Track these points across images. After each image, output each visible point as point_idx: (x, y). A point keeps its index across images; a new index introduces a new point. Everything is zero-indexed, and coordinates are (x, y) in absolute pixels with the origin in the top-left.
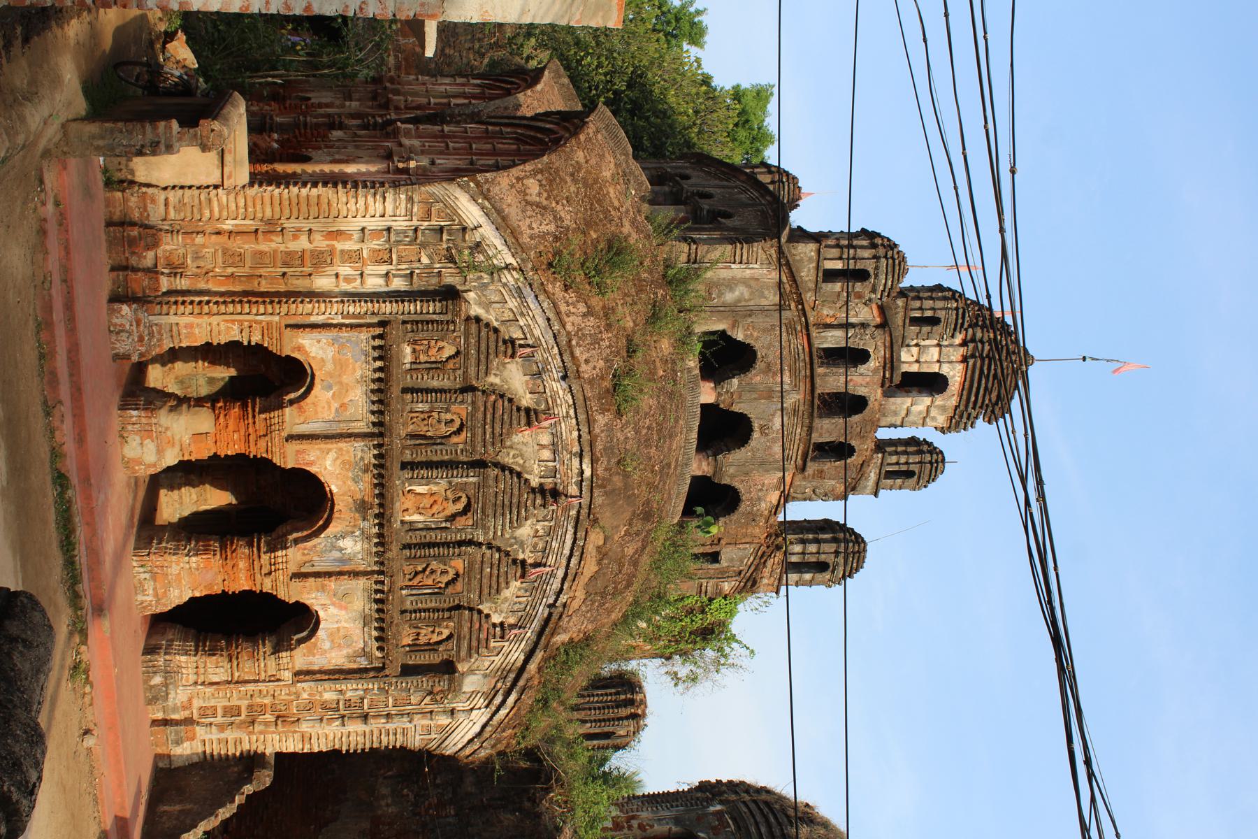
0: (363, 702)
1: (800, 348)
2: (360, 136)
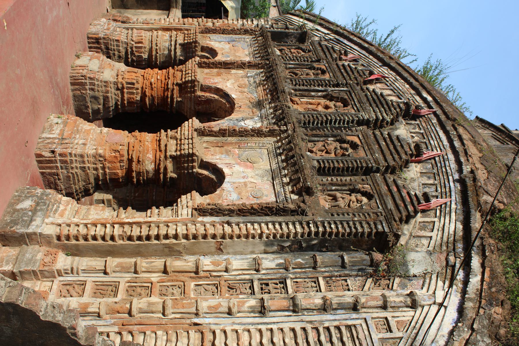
0: (285, 287)
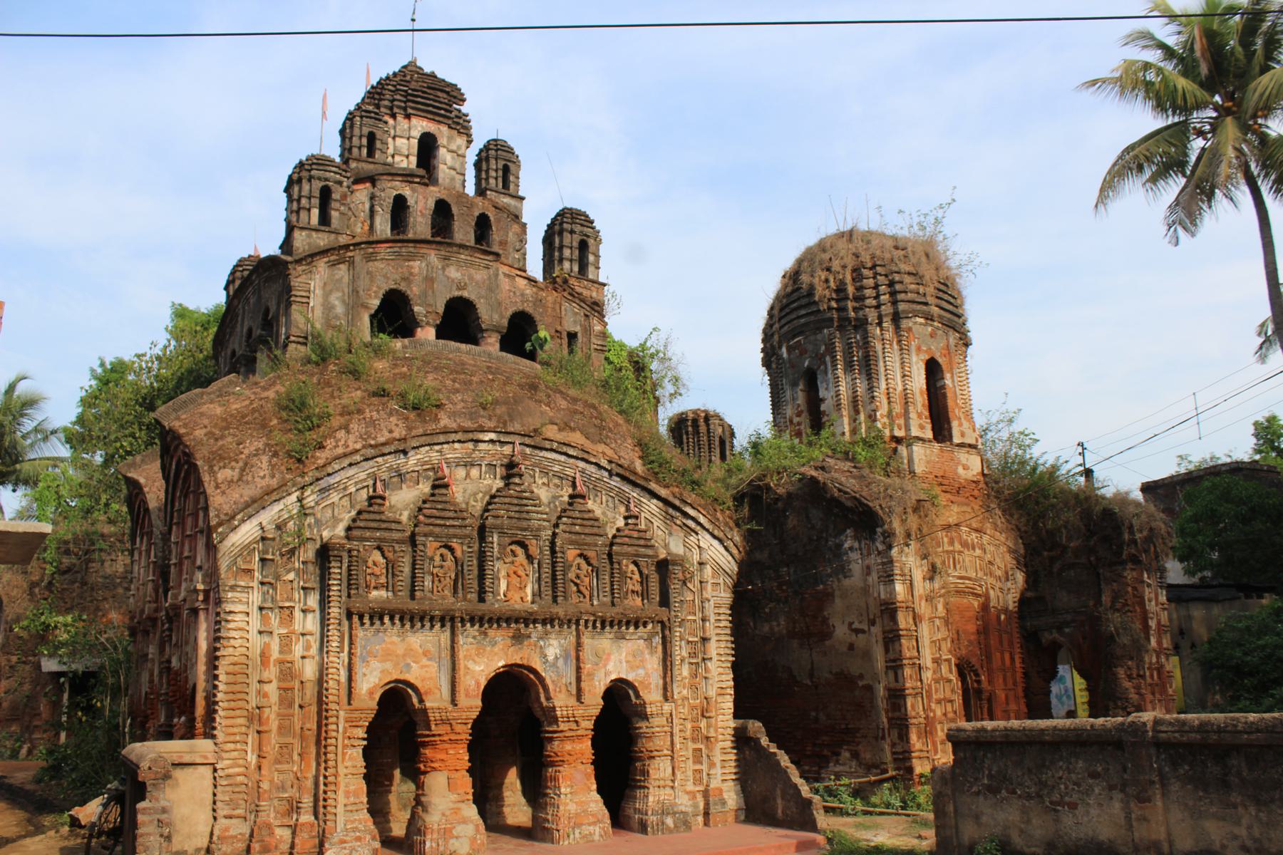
0: (691, 642)
1: (389, 250)
2: (177, 641)
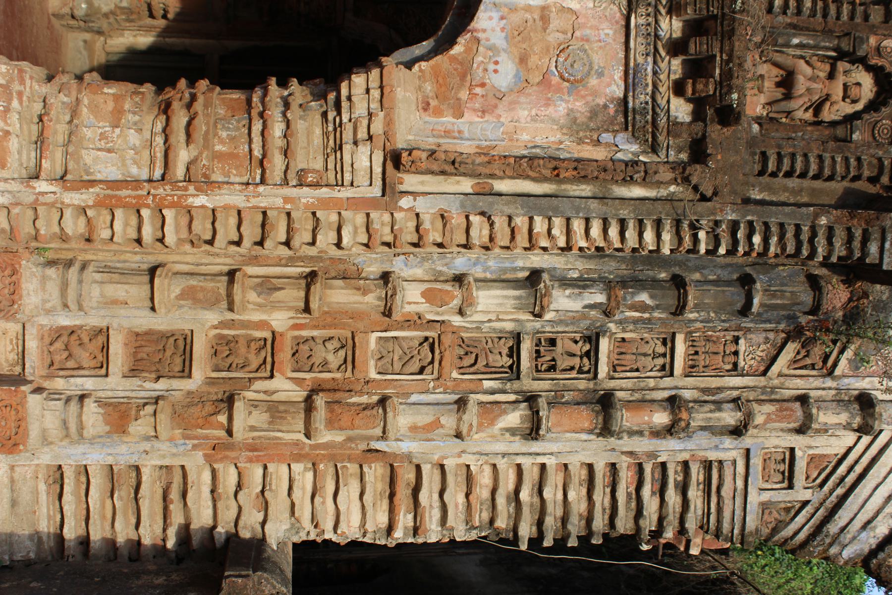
0: (592, 354)
